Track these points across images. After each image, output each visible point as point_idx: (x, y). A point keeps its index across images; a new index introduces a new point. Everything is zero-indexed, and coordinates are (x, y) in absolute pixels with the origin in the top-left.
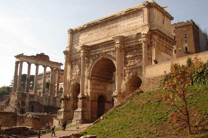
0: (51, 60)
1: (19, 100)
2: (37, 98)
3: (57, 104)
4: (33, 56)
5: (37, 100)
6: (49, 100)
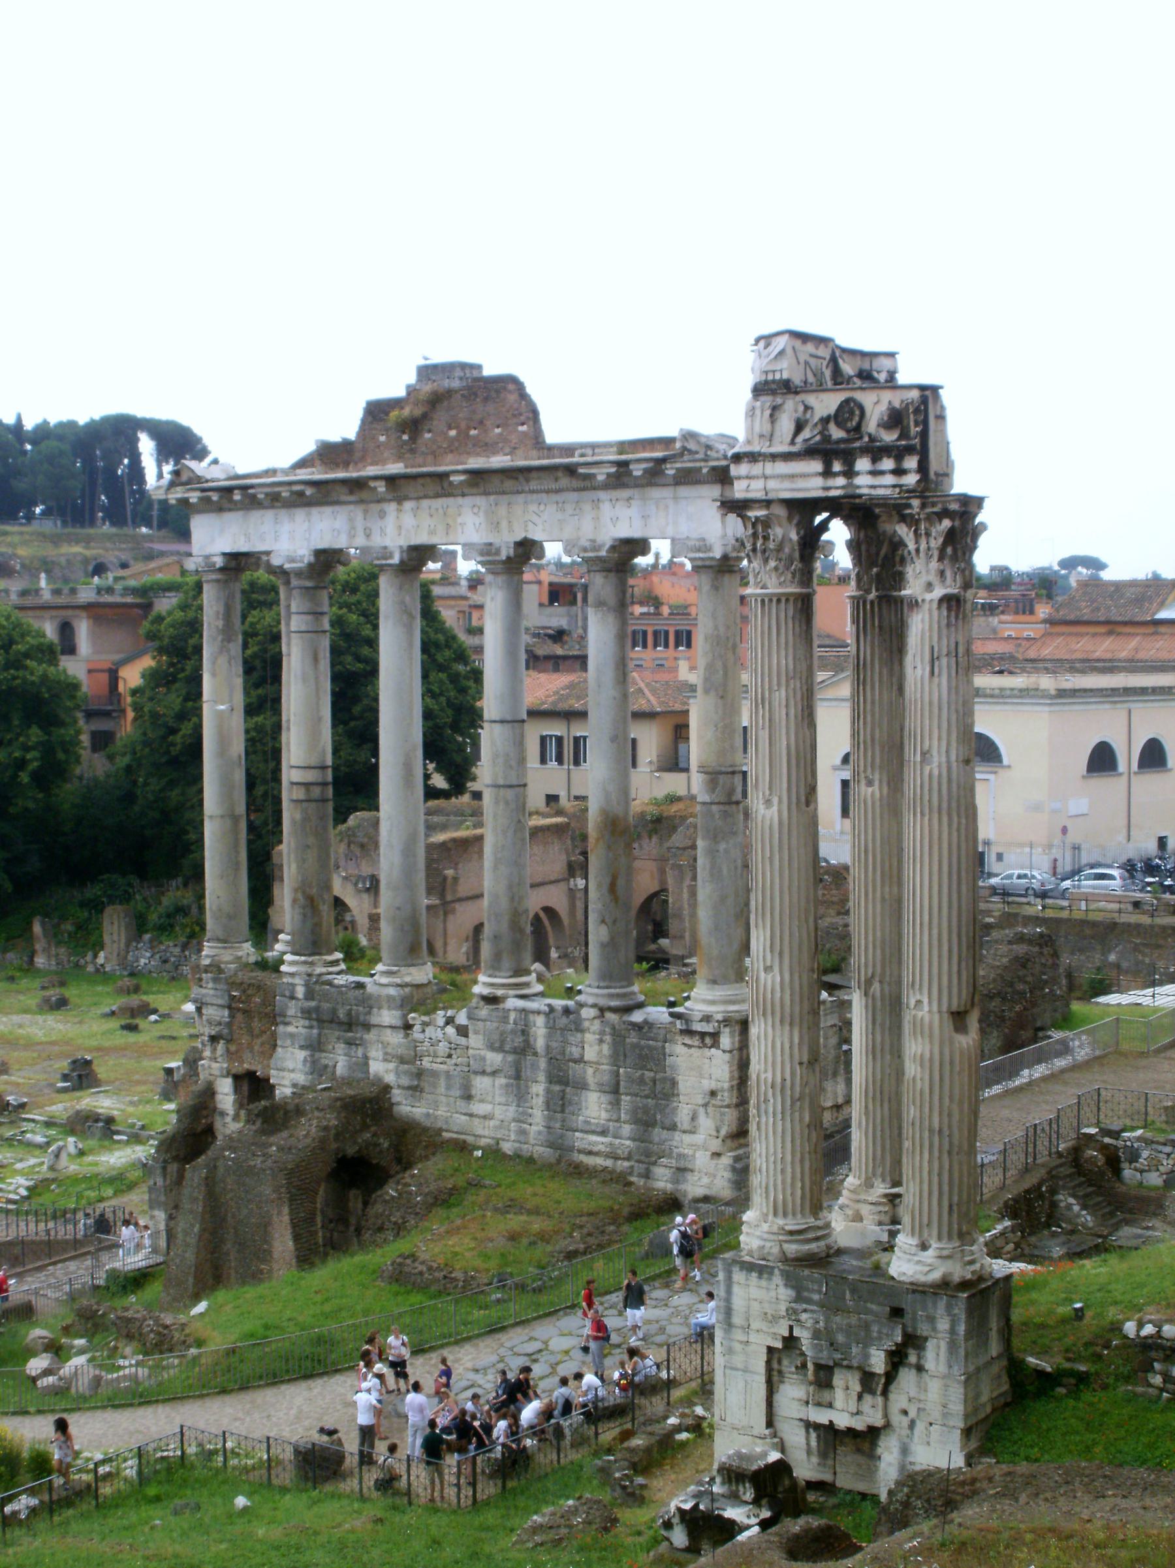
0: (569, 419)
1: (214, 1050)
2: (395, 1039)
3: (683, 1142)
4: (330, 453)
5: (402, 1060)
6: (564, 1082)
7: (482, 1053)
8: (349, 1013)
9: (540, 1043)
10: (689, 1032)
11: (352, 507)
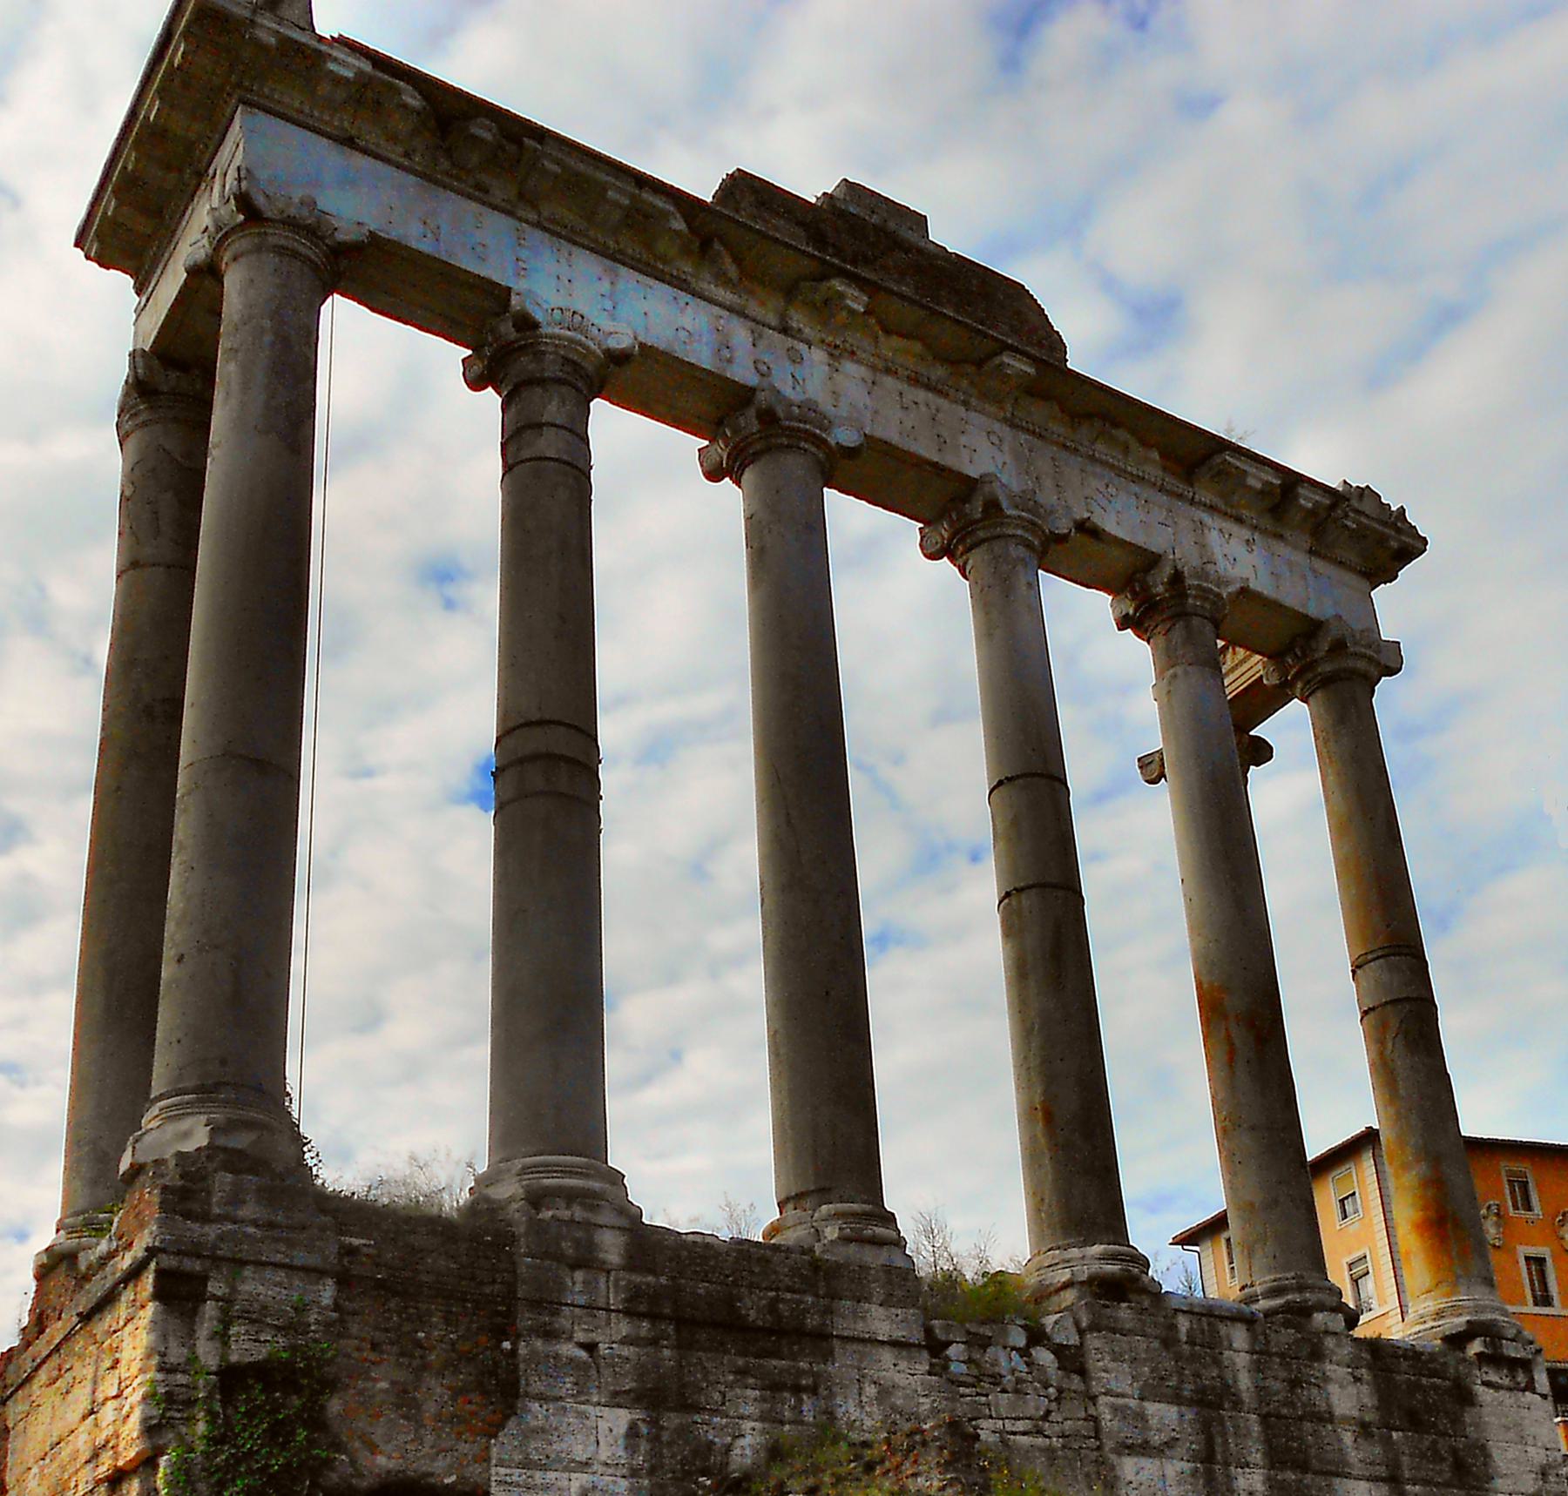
7: (1133, 1403)
8: (772, 1306)
9: (1245, 1382)
10: (1493, 1359)
11: (725, 313)
